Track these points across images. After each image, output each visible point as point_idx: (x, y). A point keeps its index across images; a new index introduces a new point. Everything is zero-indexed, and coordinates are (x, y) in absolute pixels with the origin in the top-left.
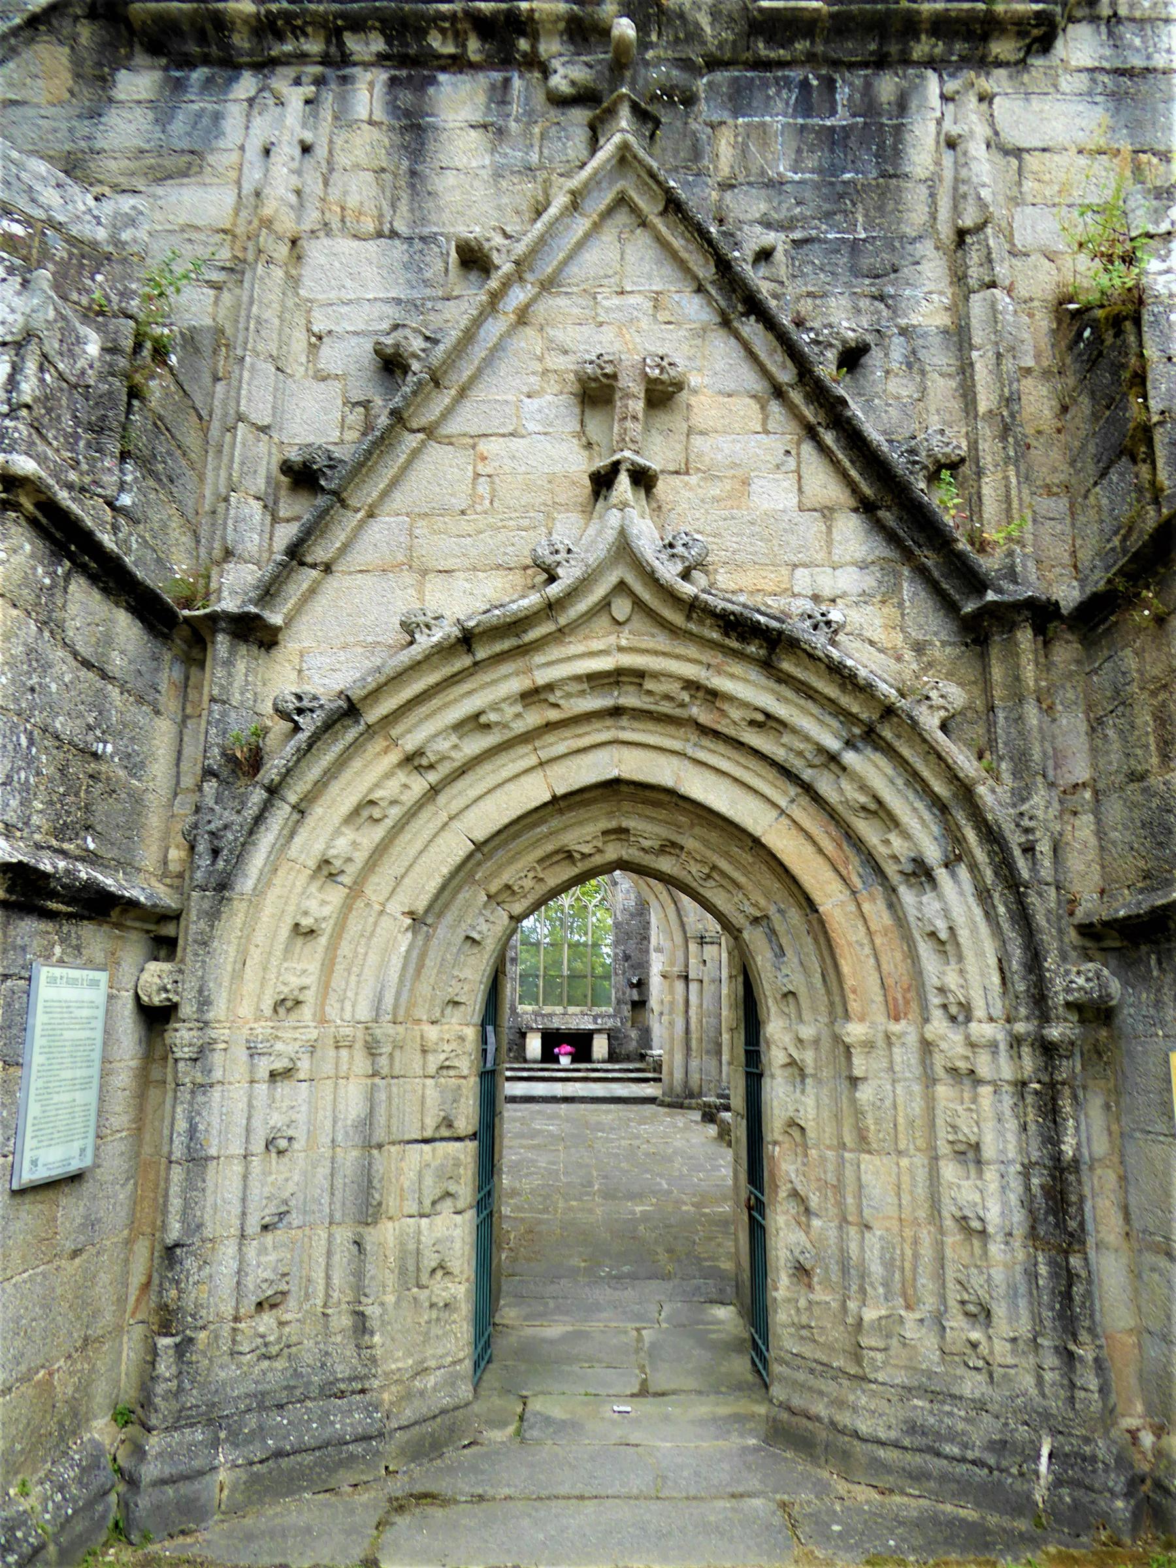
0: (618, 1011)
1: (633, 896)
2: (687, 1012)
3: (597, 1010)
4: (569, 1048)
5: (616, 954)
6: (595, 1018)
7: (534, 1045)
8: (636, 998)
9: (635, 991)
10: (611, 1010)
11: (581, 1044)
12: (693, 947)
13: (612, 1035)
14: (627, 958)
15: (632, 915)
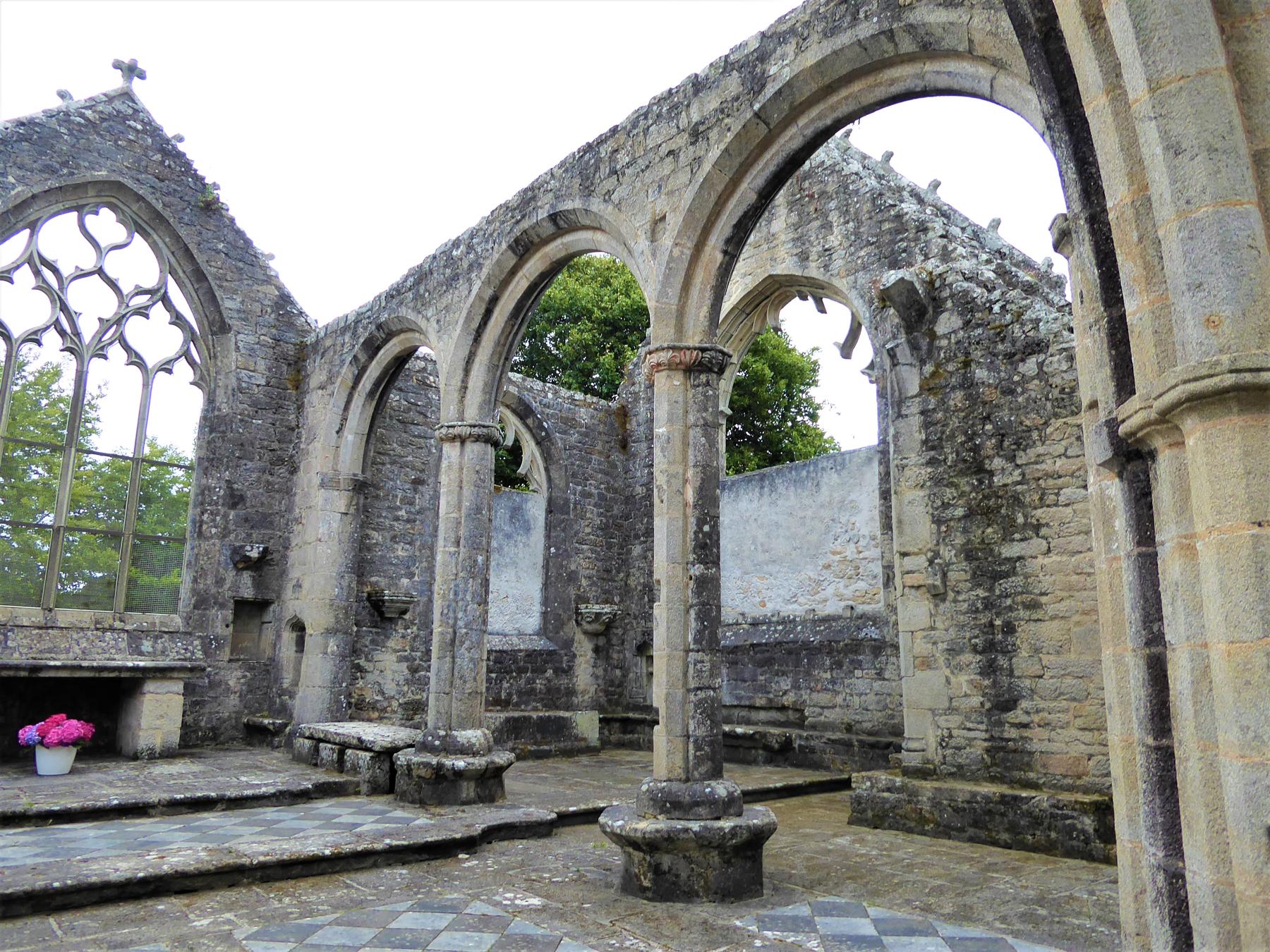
1: (262, 365)
3: (137, 620)
4: (75, 727)
5: (204, 491)
6: (135, 637)
8: (248, 592)
9: (247, 577)
10: (177, 621)
14: (235, 499)
15: (257, 407)
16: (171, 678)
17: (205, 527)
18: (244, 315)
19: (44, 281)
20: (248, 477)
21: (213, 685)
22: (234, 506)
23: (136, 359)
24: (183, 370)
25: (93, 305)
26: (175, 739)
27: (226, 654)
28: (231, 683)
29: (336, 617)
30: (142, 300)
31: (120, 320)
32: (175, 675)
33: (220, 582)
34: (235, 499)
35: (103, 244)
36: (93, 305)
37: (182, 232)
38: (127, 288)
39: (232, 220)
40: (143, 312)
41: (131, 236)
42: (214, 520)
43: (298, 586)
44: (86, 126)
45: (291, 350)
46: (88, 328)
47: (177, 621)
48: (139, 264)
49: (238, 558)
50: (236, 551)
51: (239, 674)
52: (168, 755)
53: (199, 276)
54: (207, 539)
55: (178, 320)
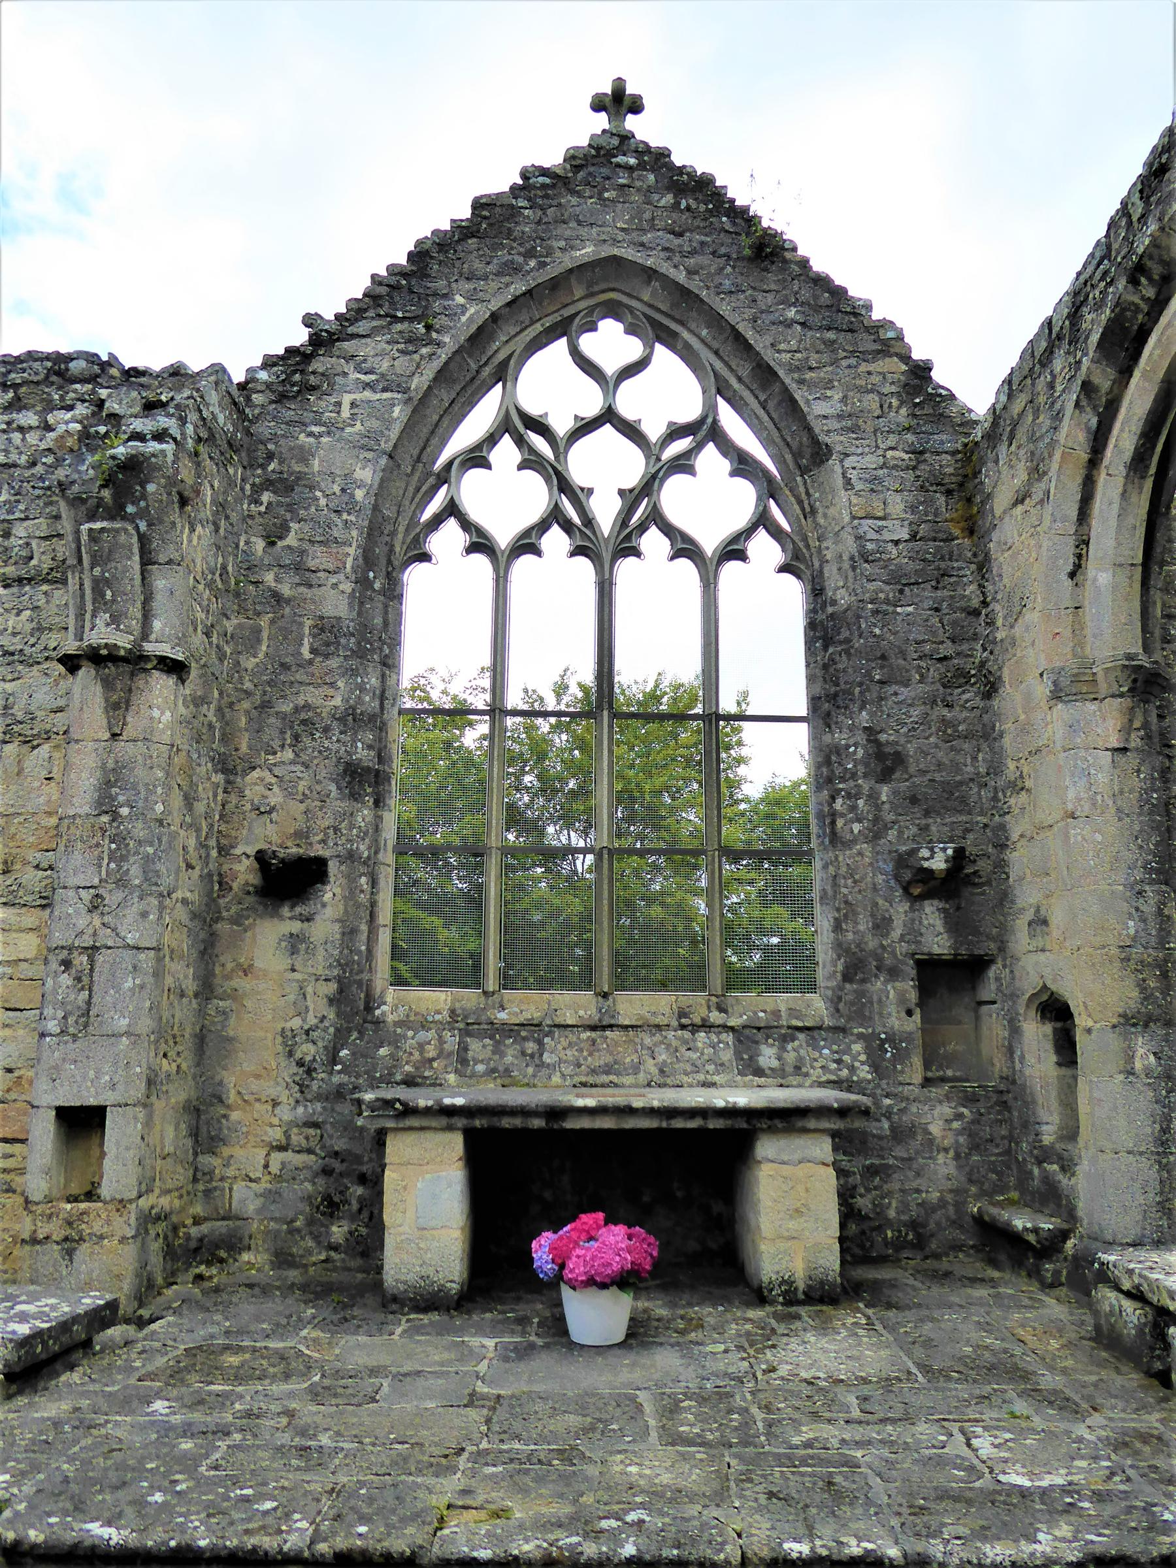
0: (852, 1011)
1: (897, 505)
4: (614, 1243)
7: (427, 1209)
8: (938, 942)
9: (932, 914)
10: (817, 1007)
11: (676, 1190)
13: (850, 1131)
14: (886, 763)
15: (901, 582)
16: (805, 1131)
17: (840, 823)
18: (852, 422)
19: (532, 450)
20: (904, 714)
21: (900, 1134)
22: (885, 776)
24: (765, 550)
25: (606, 469)
26: (831, 1261)
27: (914, 1071)
28: (936, 1129)
29: (1142, 986)
30: (682, 445)
31: (649, 486)
32: (812, 1124)
33: (882, 925)
34: (886, 763)
35: (611, 368)
36: (606, 469)
37: (724, 308)
38: (654, 431)
39: (804, 263)
40: (683, 465)
42: (853, 808)
43: (1040, 922)
44: (553, 186)
45: (947, 465)
46: (605, 511)
47: (817, 1007)
48: (668, 391)
49: (907, 875)
50: (903, 861)
51: (946, 1110)
52: (822, 1297)
53: (765, 374)
54: (848, 844)
55: (743, 465)
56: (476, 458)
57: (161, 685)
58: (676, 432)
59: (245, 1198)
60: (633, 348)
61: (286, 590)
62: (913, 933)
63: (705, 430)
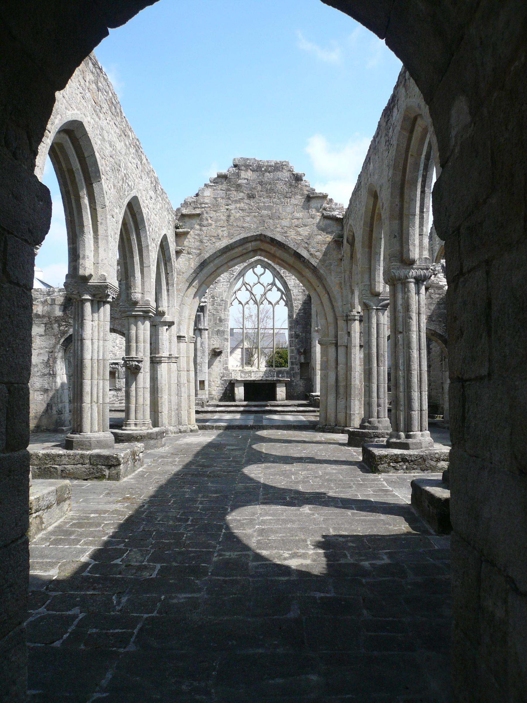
2: (336, 368)
12: (341, 323)
23: (270, 303)
24: (282, 303)
25: (258, 291)
35: (259, 274)
36: (258, 291)
38: (265, 285)
40: (270, 290)
41: (265, 271)
46: (258, 298)
55: (279, 289)
56: (239, 289)
57: (206, 332)
58: (269, 284)
59: (214, 393)
60: (263, 269)
61: (215, 313)
62: (300, 360)
63: (273, 284)
